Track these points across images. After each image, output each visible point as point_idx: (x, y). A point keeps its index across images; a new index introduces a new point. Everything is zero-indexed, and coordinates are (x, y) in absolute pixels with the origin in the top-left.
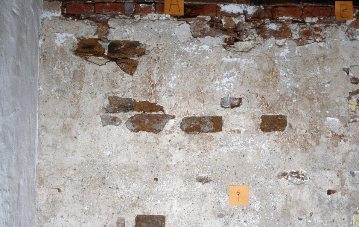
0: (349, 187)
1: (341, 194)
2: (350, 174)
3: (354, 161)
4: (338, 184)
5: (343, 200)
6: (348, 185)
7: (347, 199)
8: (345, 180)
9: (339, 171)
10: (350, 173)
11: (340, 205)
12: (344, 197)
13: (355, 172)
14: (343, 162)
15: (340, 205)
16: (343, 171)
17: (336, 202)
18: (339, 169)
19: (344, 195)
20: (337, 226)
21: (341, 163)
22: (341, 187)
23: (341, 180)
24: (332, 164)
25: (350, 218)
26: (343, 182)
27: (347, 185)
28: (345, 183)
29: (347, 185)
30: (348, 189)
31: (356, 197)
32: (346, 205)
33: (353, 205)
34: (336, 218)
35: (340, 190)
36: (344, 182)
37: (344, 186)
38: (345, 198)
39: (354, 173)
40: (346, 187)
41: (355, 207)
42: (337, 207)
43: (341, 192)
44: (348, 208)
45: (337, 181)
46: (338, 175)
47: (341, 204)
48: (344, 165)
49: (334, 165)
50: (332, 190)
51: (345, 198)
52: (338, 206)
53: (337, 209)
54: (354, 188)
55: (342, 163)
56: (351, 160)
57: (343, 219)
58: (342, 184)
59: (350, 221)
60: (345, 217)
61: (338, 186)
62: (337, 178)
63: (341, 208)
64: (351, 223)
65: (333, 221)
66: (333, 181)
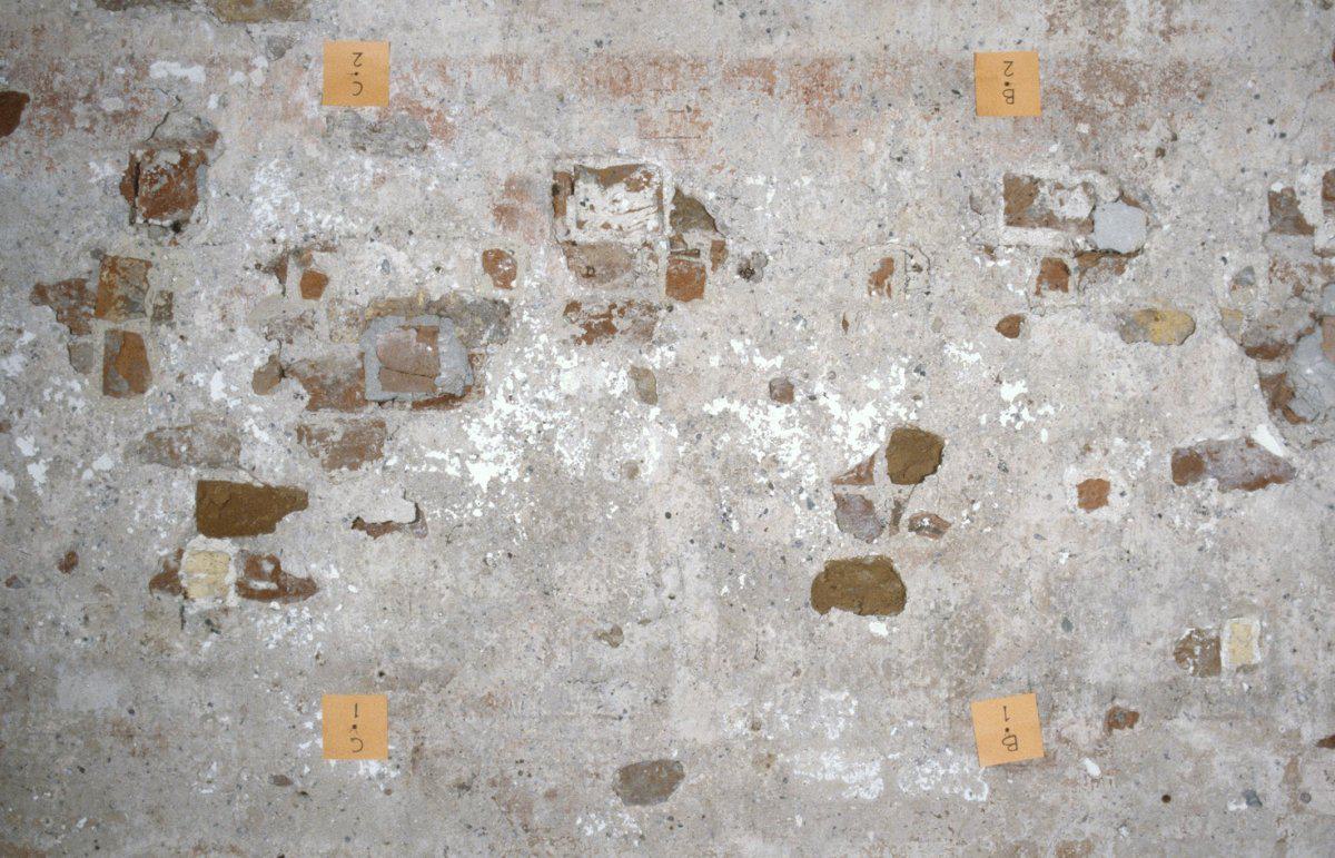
0: (1271, 759)
1: (1299, 736)
2: (1262, 800)
3: (1246, 843)
4: (1309, 768)
5: (1296, 715)
6: (1270, 766)
7: (1282, 719)
8: (1284, 782)
9: (1299, 810)
10: (1261, 804)
11: (1302, 699)
12: (1292, 723)
13: (1244, 806)
14: (1283, 841)
15: (1302, 699)
16: (1285, 810)
17: (1319, 707)
18: (1302, 818)
19: (1290, 731)
20: (1317, 630)
21: (1290, 838)
22: (1300, 759)
23: (1298, 779)
24: (1324, 834)
25: (1274, 654)
26: (1293, 774)
27: (1278, 763)
28: (1282, 772)
29: (1278, 763)
30: (1277, 751)
31: (1249, 724)
32: (1284, 697)
33: (1258, 698)
34: (1320, 654)
35: (1304, 748)
36: (1286, 776)
37: (1289, 760)
38: (1286, 721)
39: (1248, 803)
40: (1281, 760)
41: (1252, 691)
42: (1316, 692)
43: (1302, 742)
44: (1277, 686)
45: (1311, 780)
46: (1306, 797)
47: (1300, 703)
48: (1280, 831)
49: (1318, 830)
50: (1330, 750)
51: (1286, 721)
52: (1312, 694)
53: (1314, 685)
54: (1254, 753)
55: (1286, 836)
56: (1253, 845)
57: (1295, 651)
58: (1296, 768)
59: (1273, 645)
60: (1288, 659)
61: (1308, 761)
62: (1310, 788)
63: (1300, 689)
64: (1269, 637)
65: (1329, 645)
66: (1325, 777)
